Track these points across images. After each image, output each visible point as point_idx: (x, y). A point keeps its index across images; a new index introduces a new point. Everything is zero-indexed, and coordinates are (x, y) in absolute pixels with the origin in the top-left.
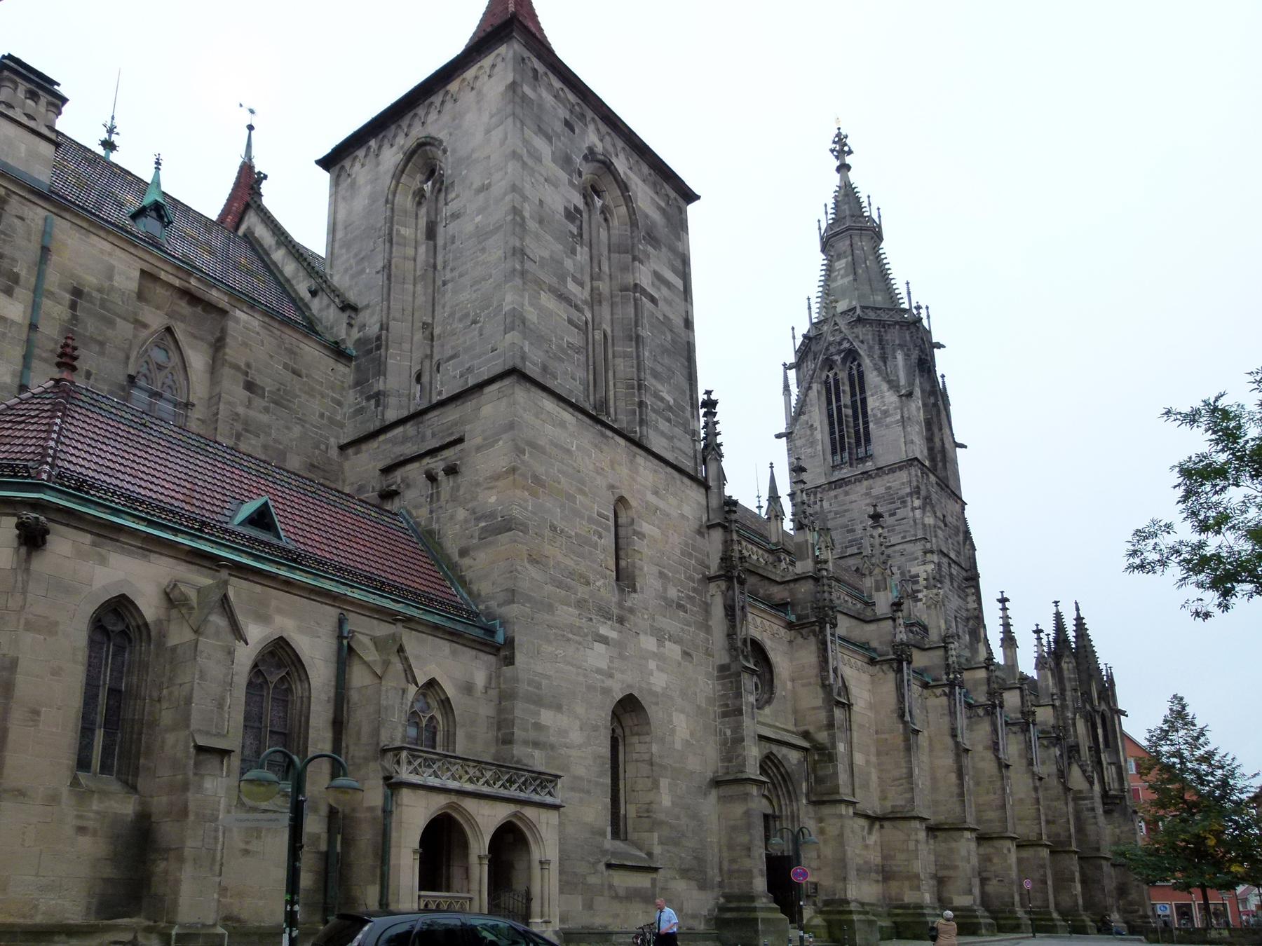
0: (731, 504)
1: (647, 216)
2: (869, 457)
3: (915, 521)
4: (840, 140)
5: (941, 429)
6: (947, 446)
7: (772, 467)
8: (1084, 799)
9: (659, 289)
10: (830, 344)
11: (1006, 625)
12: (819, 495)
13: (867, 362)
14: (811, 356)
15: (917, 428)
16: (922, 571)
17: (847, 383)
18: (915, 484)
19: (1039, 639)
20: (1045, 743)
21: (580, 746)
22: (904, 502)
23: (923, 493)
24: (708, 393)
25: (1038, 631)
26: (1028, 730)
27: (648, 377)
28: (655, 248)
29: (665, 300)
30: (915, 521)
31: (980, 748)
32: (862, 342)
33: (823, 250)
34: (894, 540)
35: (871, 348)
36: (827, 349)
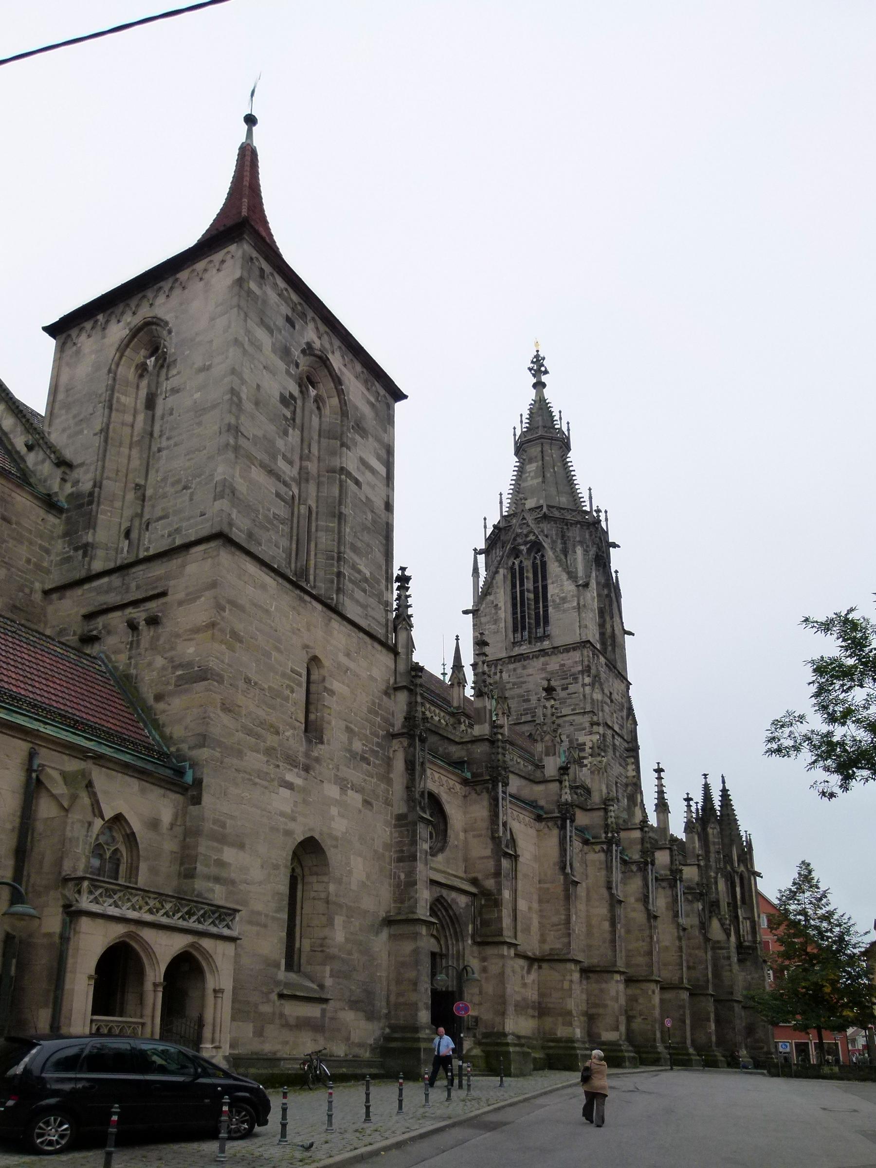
0: (417, 670)
1: (357, 408)
2: (546, 636)
3: (584, 696)
4: (538, 361)
5: (612, 618)
6: (617, 632)
7: (457, 639)
8: (721, 948)
9: (363, 473)
10: (518, 535)
11: (661, 793)
12: (499, 667)
14: (499, 545)
16: (588, 740)
17: (531, 571)
18: (586, 663)
19: (689, 806)
20: (690, 897)
21: (260, 883)
23: (593, 671)
24: (403, 569)
25: (688, 800)
26: (675, 886)
27: (348, 550)
28: (362, 437)
29: (369, 484)
30: (584, 696)
31: (632, 900)
33: (516, 454)
34: (566, 711)
36: (515, 539)
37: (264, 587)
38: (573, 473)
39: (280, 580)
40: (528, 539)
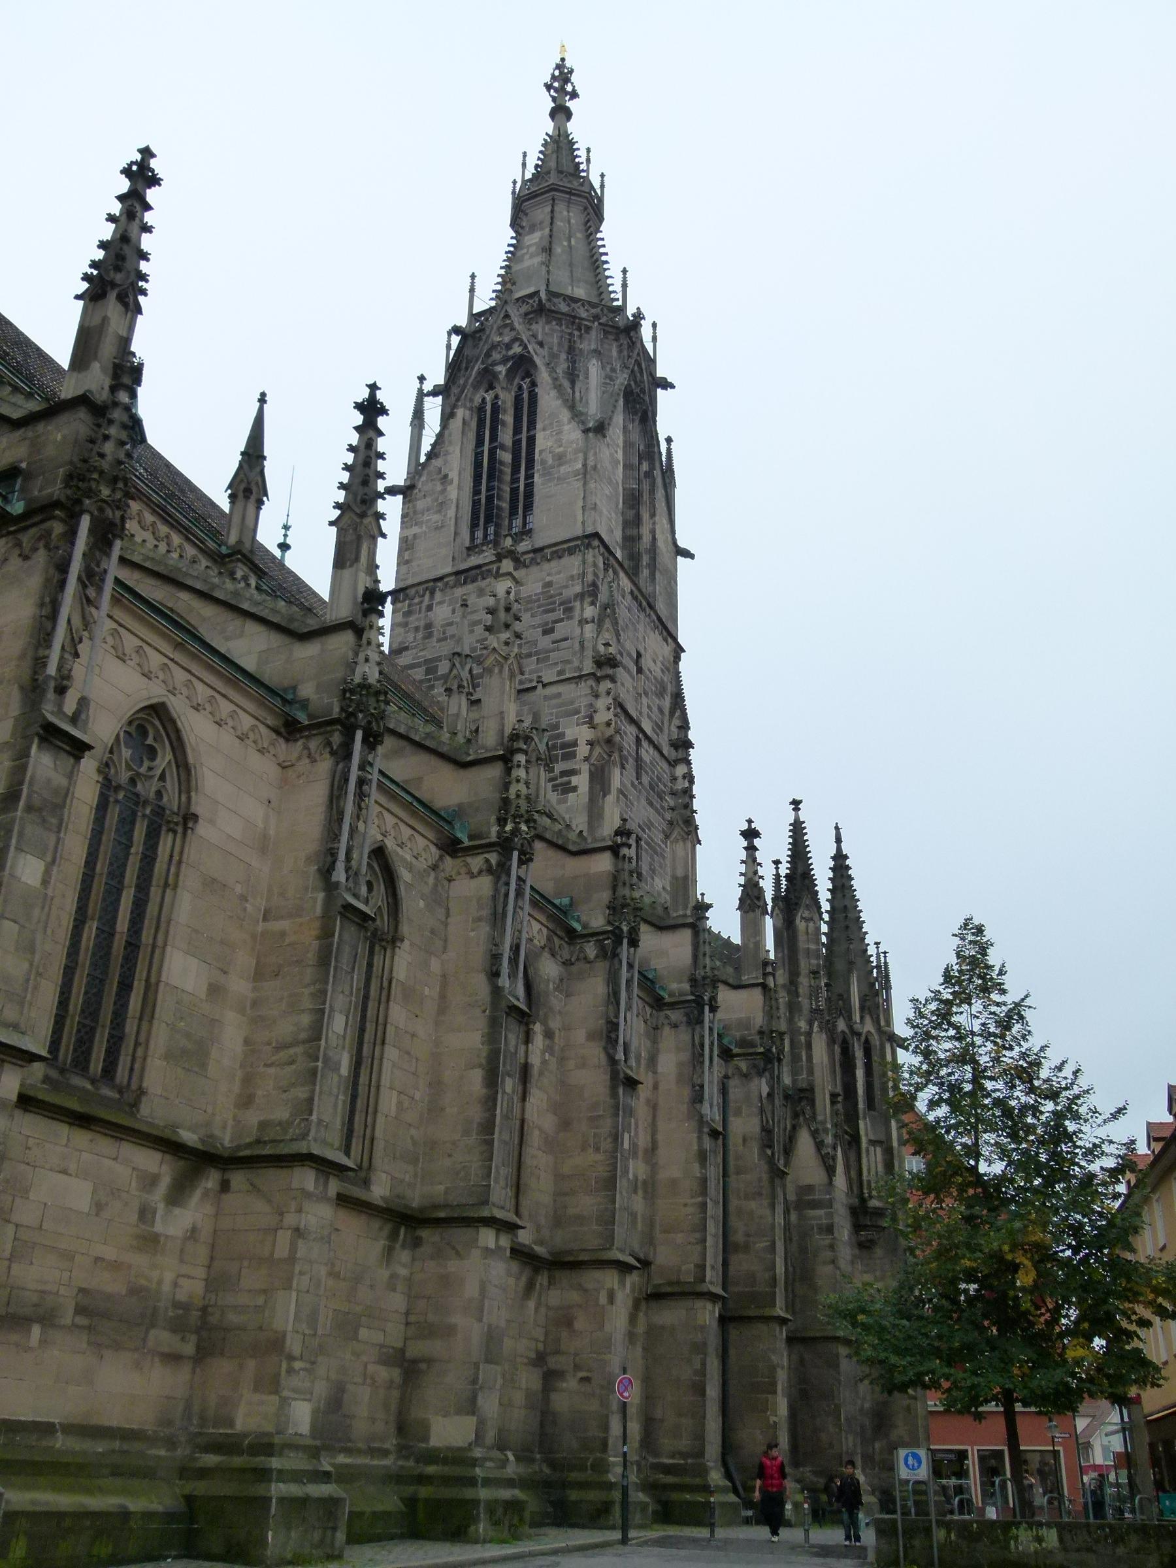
3: (582, 644)
8: (815, 1205)
10: (494, 347)
13: (543, 376)
15: (608, 490)
17: (511, 411)
18: (590, 578)
22: (569, 610)
23: (603, 597)
30: (582, 644)
32: (541, 344)
35: (553, 356)
38: (604, 258)
40: (511, 353)
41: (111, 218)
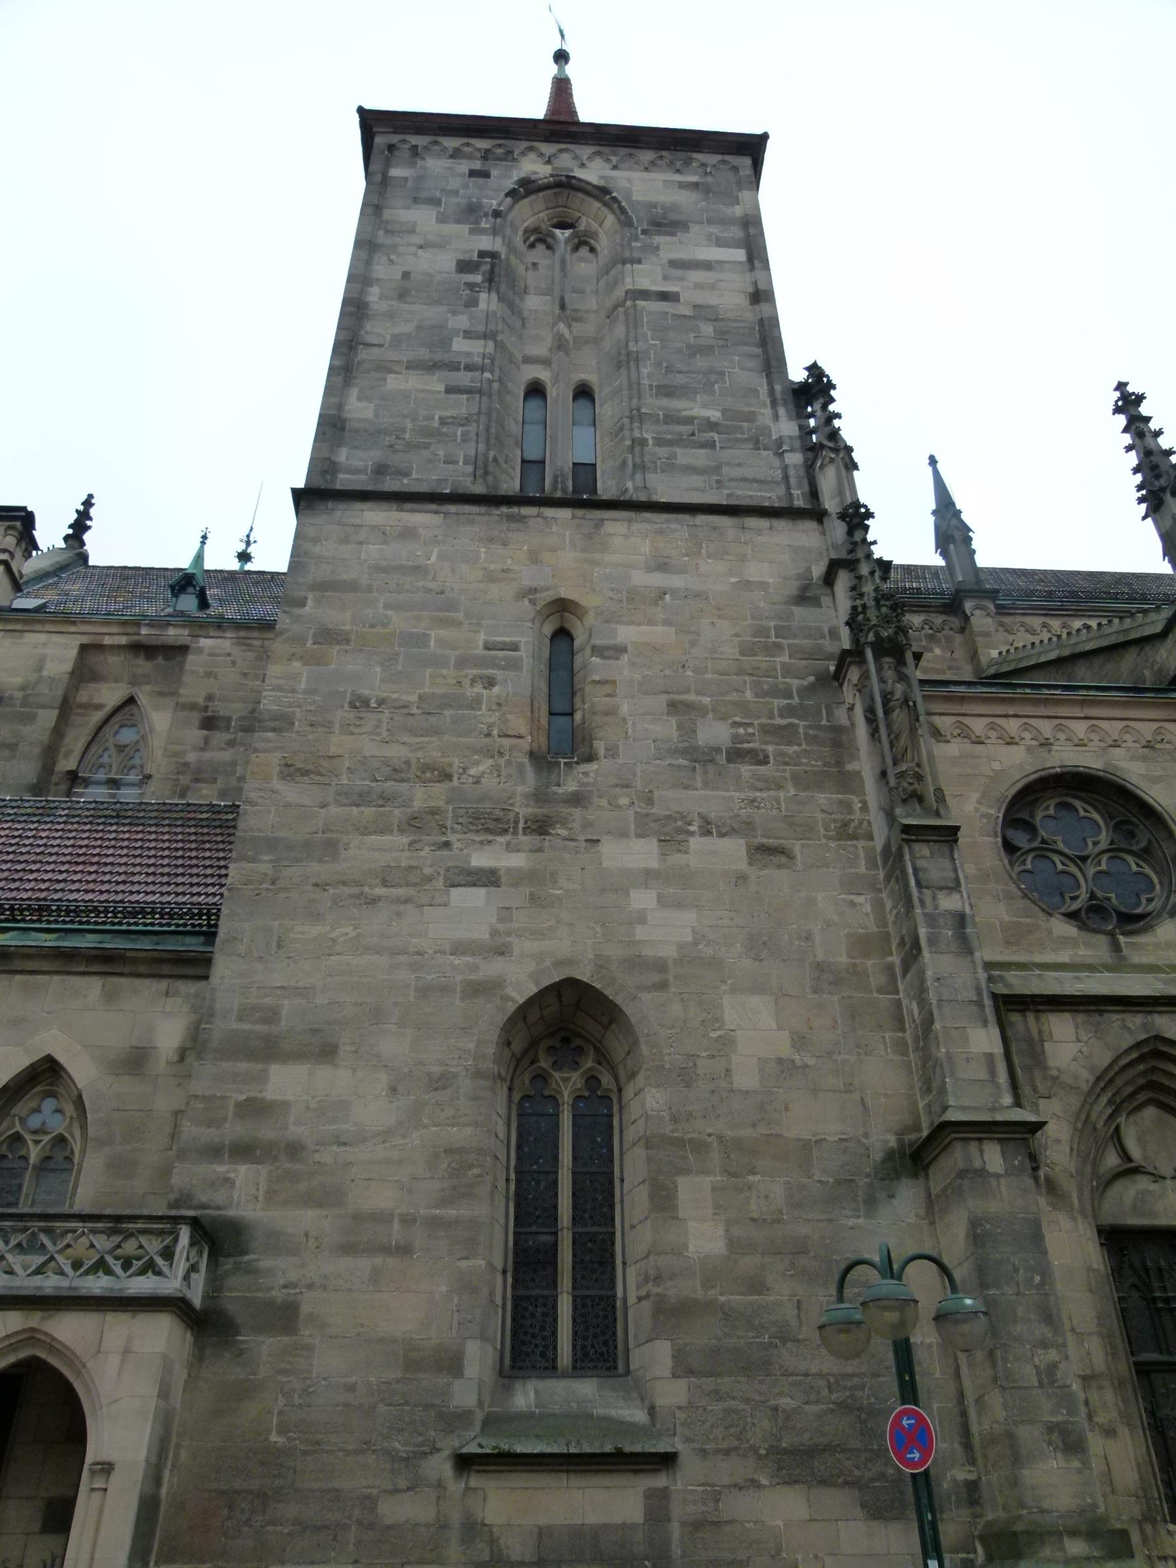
21: (386, 1135)
37: (408, 534)
39: (452, 508)
41: (1129, 448)
